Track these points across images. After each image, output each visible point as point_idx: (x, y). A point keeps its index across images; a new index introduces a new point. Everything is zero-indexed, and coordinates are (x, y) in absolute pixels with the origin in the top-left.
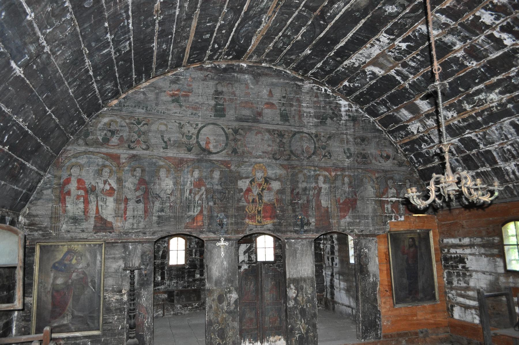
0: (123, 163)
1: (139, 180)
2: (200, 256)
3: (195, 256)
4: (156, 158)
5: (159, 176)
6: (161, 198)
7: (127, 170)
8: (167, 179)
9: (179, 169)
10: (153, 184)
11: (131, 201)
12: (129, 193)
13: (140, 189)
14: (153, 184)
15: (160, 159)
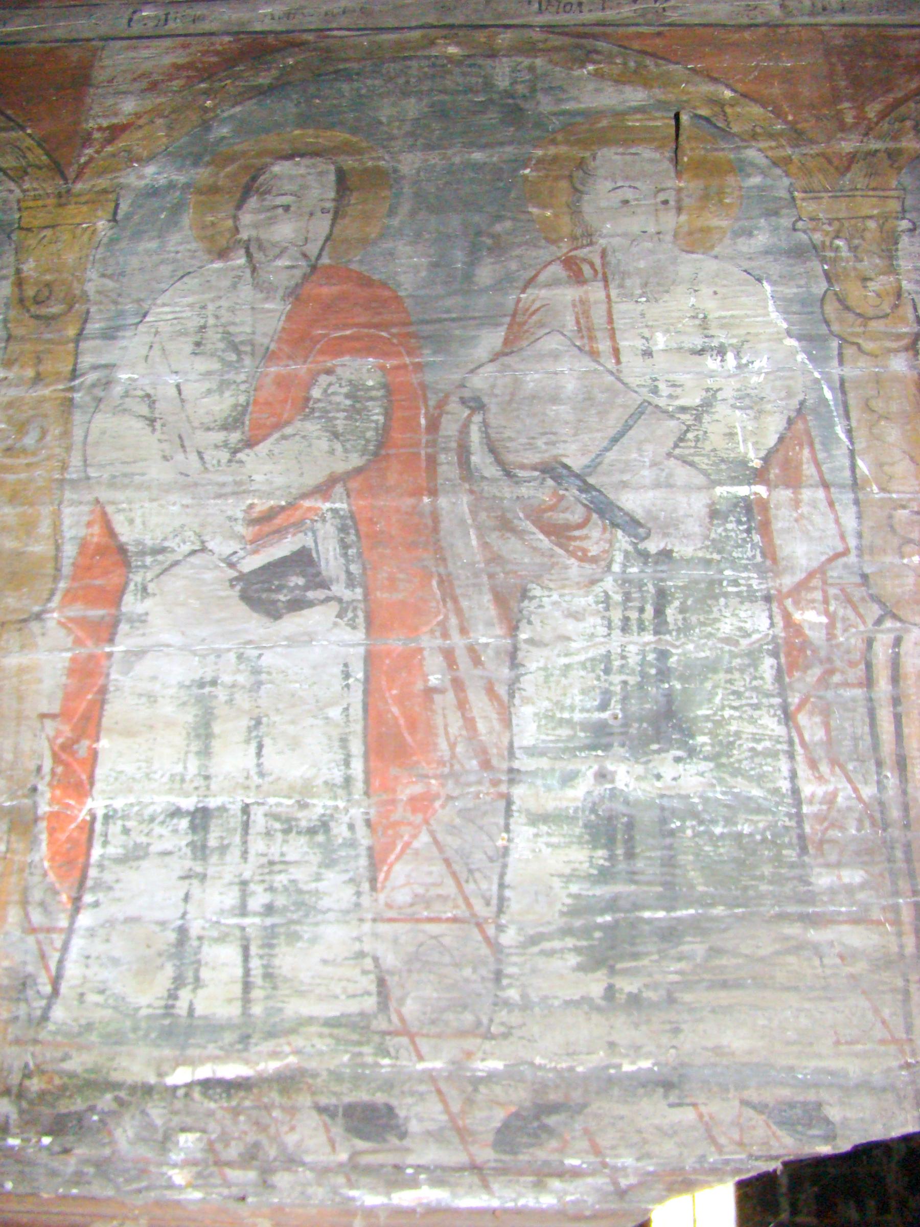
0: (116, 132)
1: (295, 294)
2: (820, 1214)
3: (794, 1212)
4: (531, 49)
5: (589, 236)
6: (632, 525)
7: (153, 192)
8: (688, 264)
9: (848, 145)
10: (492, 339)
11: (175, 583)
12: (158, 472)
13: (305, 408)
14: (492, 339)
15: (589, 56)
